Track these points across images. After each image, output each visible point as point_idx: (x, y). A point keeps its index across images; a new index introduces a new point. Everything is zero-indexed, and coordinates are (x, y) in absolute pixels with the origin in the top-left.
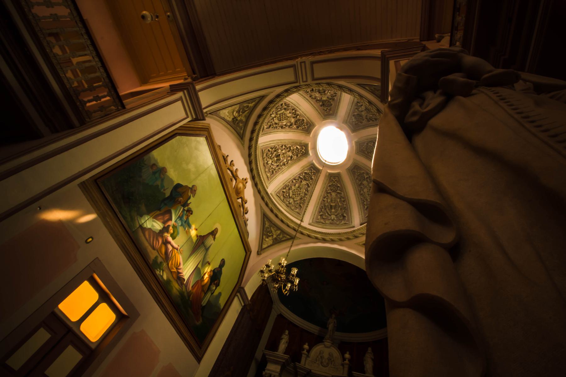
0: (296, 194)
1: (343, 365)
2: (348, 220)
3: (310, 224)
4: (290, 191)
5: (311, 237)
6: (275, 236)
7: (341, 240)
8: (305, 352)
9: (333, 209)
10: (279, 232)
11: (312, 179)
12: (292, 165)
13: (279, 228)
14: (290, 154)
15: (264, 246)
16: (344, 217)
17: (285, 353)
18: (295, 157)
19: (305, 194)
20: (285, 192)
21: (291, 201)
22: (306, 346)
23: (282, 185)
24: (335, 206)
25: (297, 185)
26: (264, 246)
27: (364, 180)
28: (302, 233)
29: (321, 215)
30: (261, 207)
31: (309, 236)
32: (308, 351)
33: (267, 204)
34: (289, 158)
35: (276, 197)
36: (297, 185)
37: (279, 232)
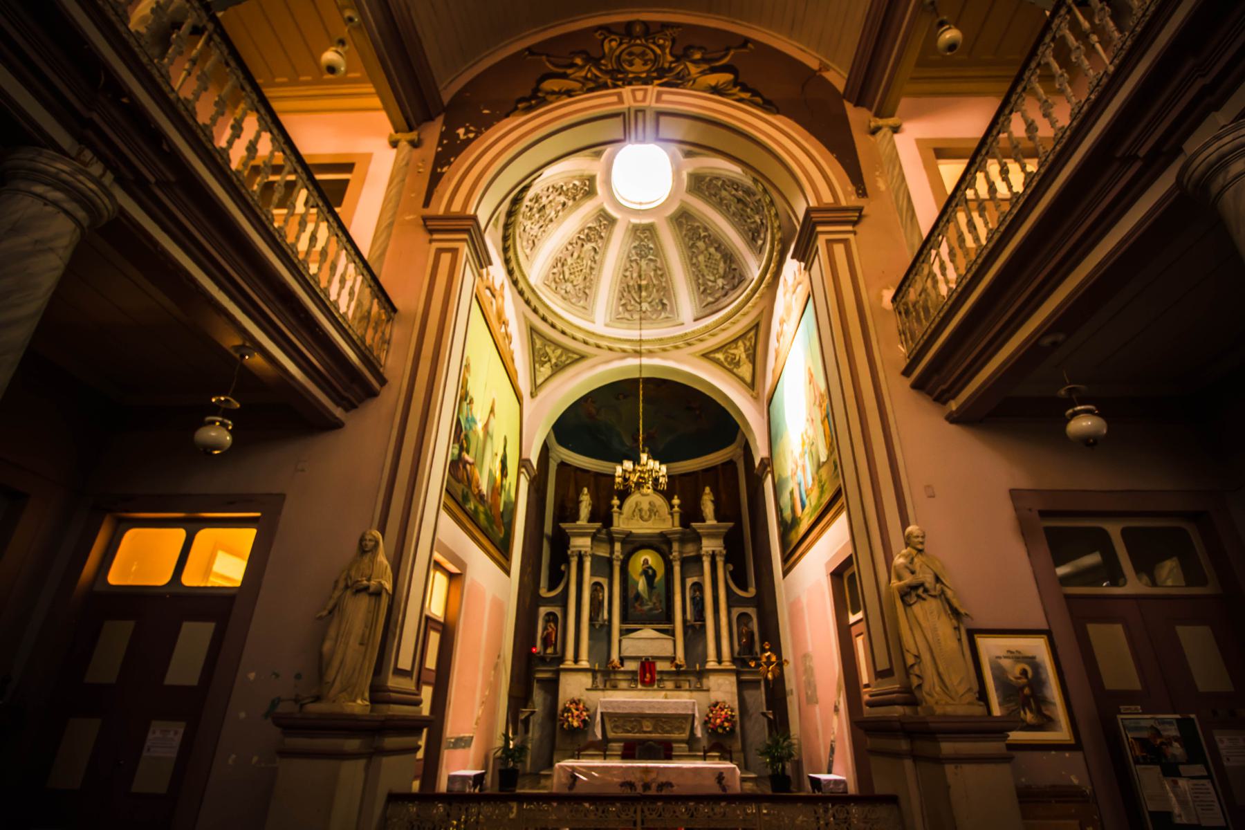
0: (574, 274)
1: (672, 514)
2: (672, 311)
3: (606, 325)
4: (566, 269)
5: (615, 350)
6: (554, 361)
7: (664, 350)
8: (615, 509)
9: (644, 292)
10: (559, 352)
11: (601, 237)
12: (565, 217)
13: (557, 345)
14: (562, 199)
15: (539, 381)
16: (664, 305)
17: (591, 520)
18: (570, 203)
19: (592, 268)
20: (559, 273)
21: (569, 287)
22: (616, 502)
23: (550, 262)
24: (647, 287)
25: (576, 255)
26: (539, 381)
27: (699, 238)
28: (598, 347)
29: (624, 305)
30: (525, 317)
31: (610, 349)
32: (620, 507)
33: (535, 311)
34: (560, 207)
35: (544, 289)
36: (576, 255)
37: (559, 352)
